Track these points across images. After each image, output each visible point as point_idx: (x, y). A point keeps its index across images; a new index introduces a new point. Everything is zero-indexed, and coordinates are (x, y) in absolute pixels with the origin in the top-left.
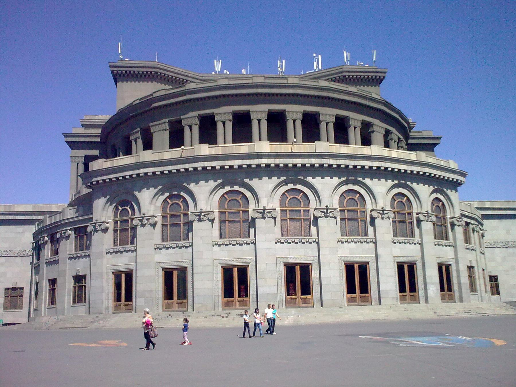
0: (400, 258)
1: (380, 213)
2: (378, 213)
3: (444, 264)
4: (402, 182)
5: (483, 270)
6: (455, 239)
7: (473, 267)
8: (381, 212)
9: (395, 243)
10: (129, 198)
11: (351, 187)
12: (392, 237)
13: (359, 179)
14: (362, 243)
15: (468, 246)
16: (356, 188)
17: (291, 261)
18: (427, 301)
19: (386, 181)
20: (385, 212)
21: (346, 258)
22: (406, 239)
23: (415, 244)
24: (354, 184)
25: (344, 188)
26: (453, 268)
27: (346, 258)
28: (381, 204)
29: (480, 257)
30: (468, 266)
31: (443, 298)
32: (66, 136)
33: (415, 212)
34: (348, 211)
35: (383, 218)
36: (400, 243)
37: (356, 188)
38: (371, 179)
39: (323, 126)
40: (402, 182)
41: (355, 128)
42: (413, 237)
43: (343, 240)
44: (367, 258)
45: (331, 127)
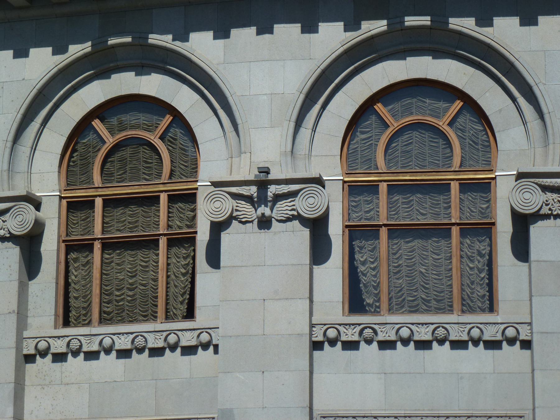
1: (249, 199)
2: (236, 196)
4: (411, 21)
8: (253, 190)
11: (126, 83)
13: (155, 39)
14: (157, 352)
16: (153, 85)
19: (310, 28)
20: (273, 190)
23: (493, 345)
24: (142, 69)
25: (95, 93)
28: (267, 147)
33: (504, 175)
34: (110, 203)
35: (265, 223)
36: (386, 345)
37: (153, 85)
38: (222, 33)
40: (411, 21)
42: (492, 309)
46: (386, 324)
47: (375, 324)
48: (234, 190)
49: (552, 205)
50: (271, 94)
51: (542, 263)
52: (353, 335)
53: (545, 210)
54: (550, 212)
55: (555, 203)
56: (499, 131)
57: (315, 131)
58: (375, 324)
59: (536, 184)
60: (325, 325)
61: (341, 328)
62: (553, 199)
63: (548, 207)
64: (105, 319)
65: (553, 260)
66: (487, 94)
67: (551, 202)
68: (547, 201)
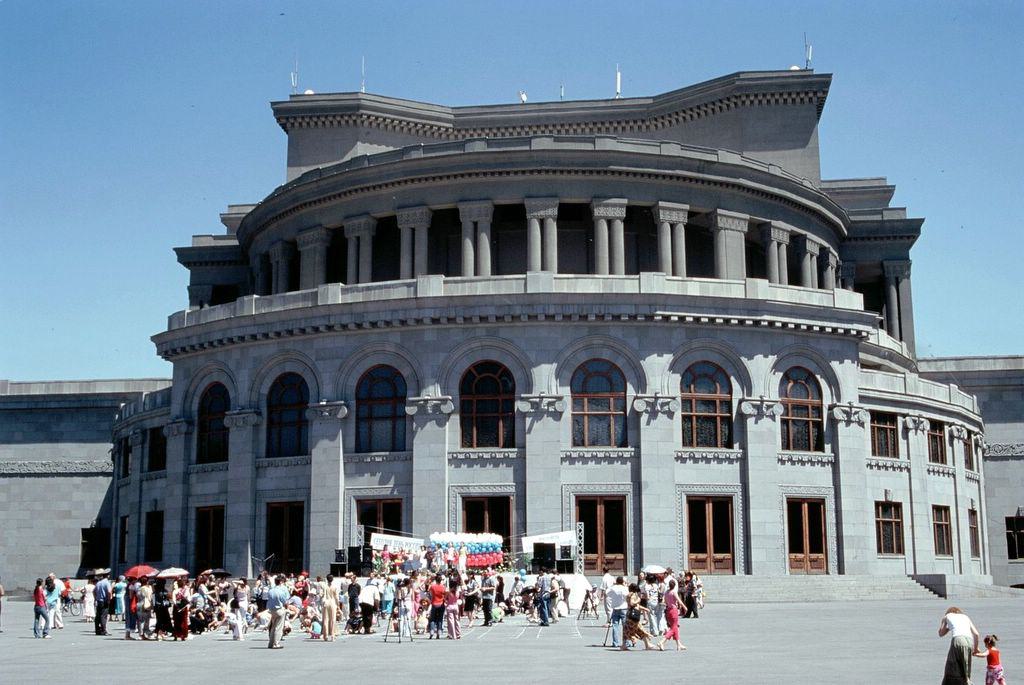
0: (695, 489)
3: (804, 500)
5: (940, 511)
6: (835, 450)
7: (898, 506)
9: (683, 460)
10: (224, 380)
12: (680, 447)
15: (882, 460)
17: (475, 491)
18: (748, 571)
21: (579, 488)
22: (709, 452)
26: (830, 505)
27: (579, 488)
29: (923, 481)
30: (877, 504)
31: (795, 565)
32: (175, 249)
39: (603, 229)
41: (673, 226)
43: (574, 455)
44: (622, 487)
45: (620, 227)
64: (593, 443)
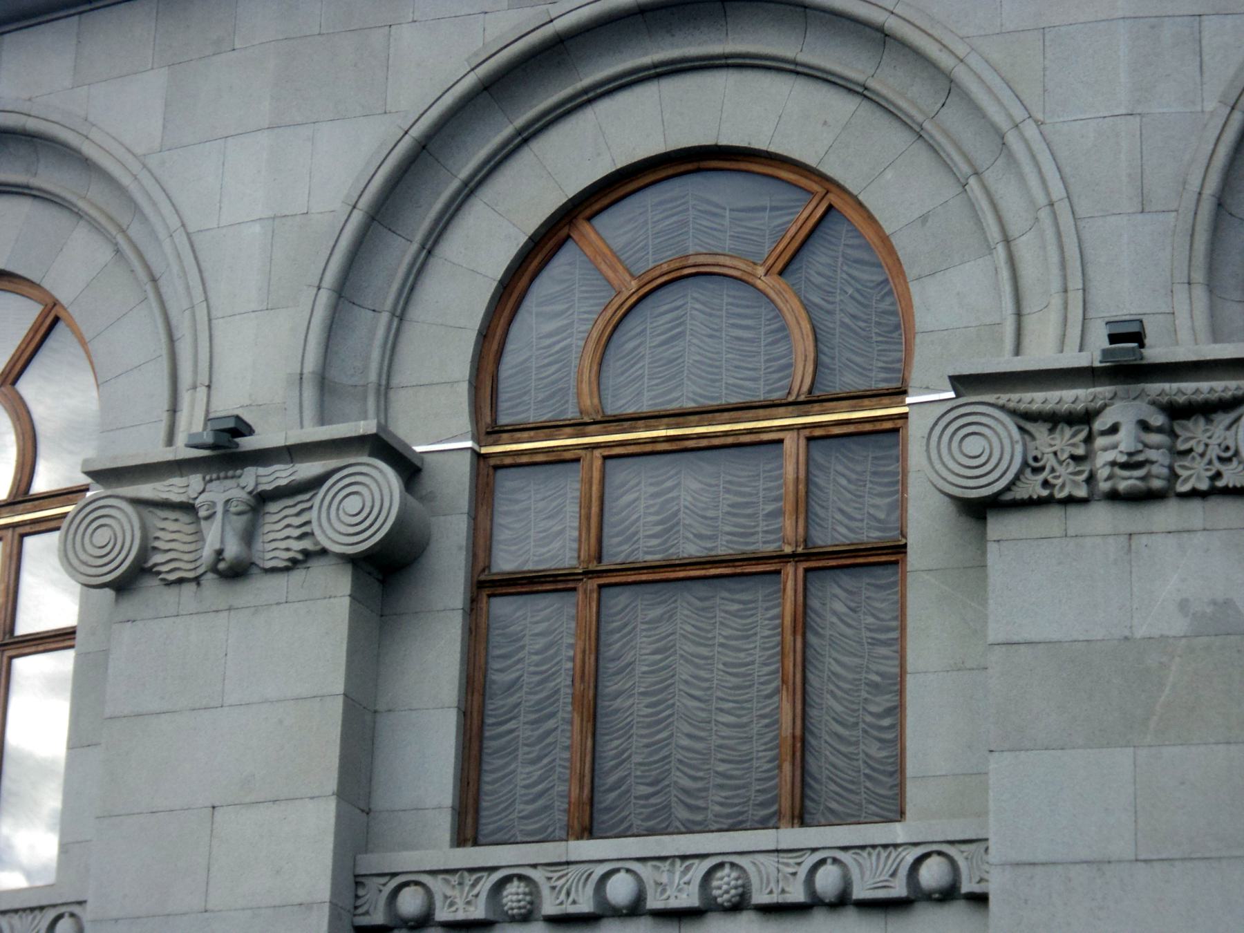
46: (568, 863)
47: (534, 866)
48: (147, 490)
49: (1053, 470)
50: (274, 218)
51: (1022, 648)
52: (468, 903)
53: (1032, 487)
54: (1045, 493)
55: (1061, 463)
56: (919, 278)
57: (401, 319)
58: (534, 866)
59: (1002, 408)
60: (394, 875)
61: (435, 884)
62: (1055, 453)
63: (1041, 477)
65: (1055, 636)
66: (889, 175)
67: (1050, 461)
68: (1036, 459)
